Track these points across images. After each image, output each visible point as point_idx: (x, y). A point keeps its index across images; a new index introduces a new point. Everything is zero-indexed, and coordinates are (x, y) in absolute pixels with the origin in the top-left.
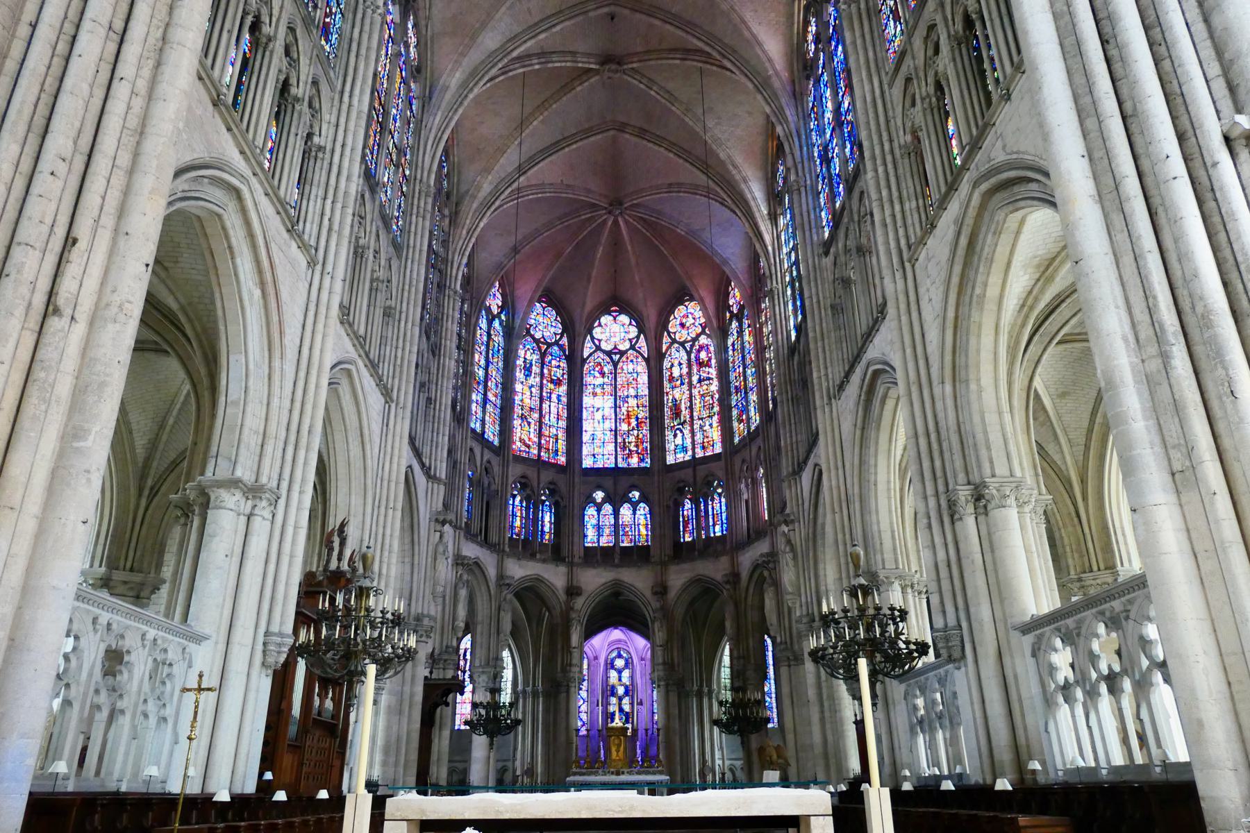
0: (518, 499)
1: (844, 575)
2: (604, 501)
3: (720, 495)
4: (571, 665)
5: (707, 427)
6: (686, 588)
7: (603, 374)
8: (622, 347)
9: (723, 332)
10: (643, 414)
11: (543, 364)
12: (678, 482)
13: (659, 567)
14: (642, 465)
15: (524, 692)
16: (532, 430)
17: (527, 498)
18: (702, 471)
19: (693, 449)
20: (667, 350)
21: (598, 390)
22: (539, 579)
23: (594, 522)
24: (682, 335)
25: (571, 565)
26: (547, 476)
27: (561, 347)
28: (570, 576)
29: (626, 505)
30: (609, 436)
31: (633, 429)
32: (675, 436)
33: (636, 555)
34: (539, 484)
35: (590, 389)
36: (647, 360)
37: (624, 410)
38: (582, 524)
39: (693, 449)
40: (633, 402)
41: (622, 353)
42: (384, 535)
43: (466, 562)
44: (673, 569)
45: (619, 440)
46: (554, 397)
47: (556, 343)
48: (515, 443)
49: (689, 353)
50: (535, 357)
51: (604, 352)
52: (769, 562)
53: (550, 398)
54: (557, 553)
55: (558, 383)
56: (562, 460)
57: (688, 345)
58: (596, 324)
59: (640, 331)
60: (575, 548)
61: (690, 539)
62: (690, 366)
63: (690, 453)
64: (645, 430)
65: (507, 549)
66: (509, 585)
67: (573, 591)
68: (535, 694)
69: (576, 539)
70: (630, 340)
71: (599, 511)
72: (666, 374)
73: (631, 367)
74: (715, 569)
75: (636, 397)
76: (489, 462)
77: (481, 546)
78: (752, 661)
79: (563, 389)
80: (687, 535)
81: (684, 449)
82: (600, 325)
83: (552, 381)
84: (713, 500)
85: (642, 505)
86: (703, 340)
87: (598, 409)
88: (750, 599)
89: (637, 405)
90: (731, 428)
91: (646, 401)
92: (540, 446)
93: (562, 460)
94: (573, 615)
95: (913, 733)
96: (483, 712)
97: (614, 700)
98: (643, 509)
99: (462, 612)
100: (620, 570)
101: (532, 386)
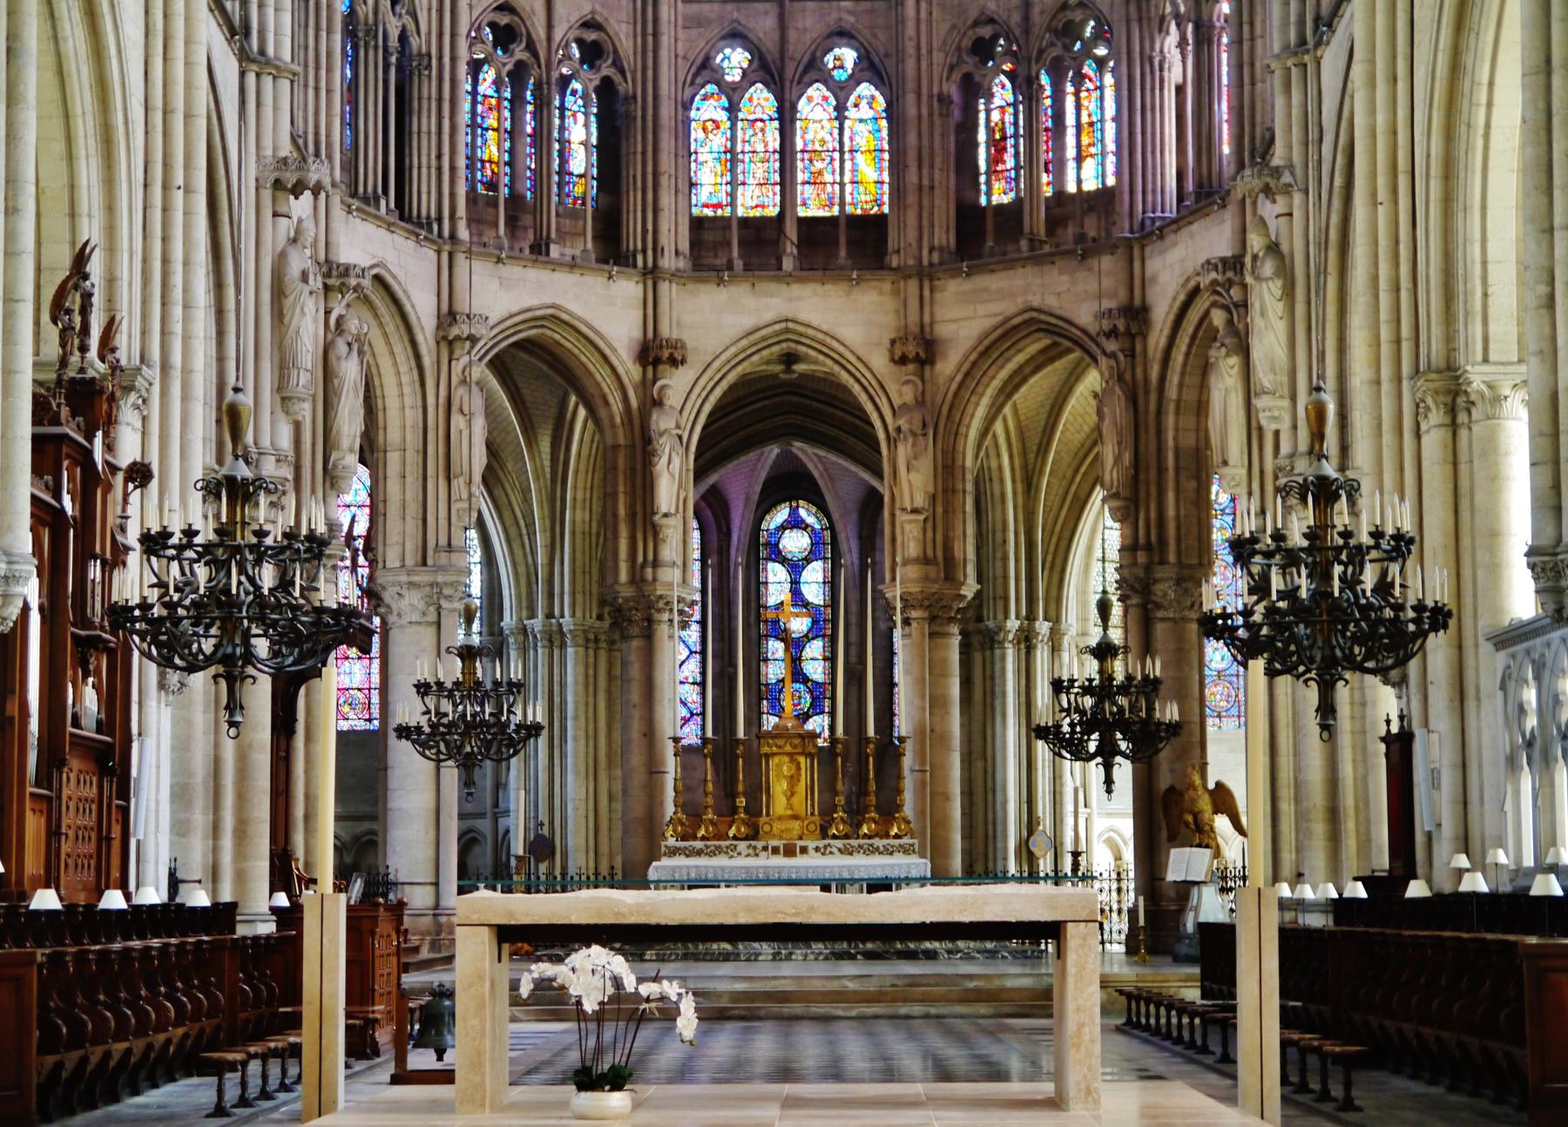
0: (488, 75)
1: (1386, 372)
2: (748, 78)
3: (1101, 63)
4: (656, 564)
12: (976, 24)
13: (913, 285)
17: (517, 76)
22: (555, 318)
23: (718, 141)
25: (652, 275)
28: (652, 308)
29: (817, 91)
34: (550, 26)
38: (686, 153)
42: (166, 261)
43: (353, 282)
52: (1230, 283)
60: (665, 224)
61: (1006, 199)
65: (463, 233)
66: (473, 339)
69: (666, 200)
71: (733, 110)
77: (390, 227)
78: (1172, 558)
80: (998, 186)
84: (1080, 78)
85: (865, 89)
88: (1174, 379)
94: (662, 422)
95: (1512, 763)
96: (446, 706)
97: (776, 648)
98: (868, 101)
99: (350, 424)
100: (796, 289)
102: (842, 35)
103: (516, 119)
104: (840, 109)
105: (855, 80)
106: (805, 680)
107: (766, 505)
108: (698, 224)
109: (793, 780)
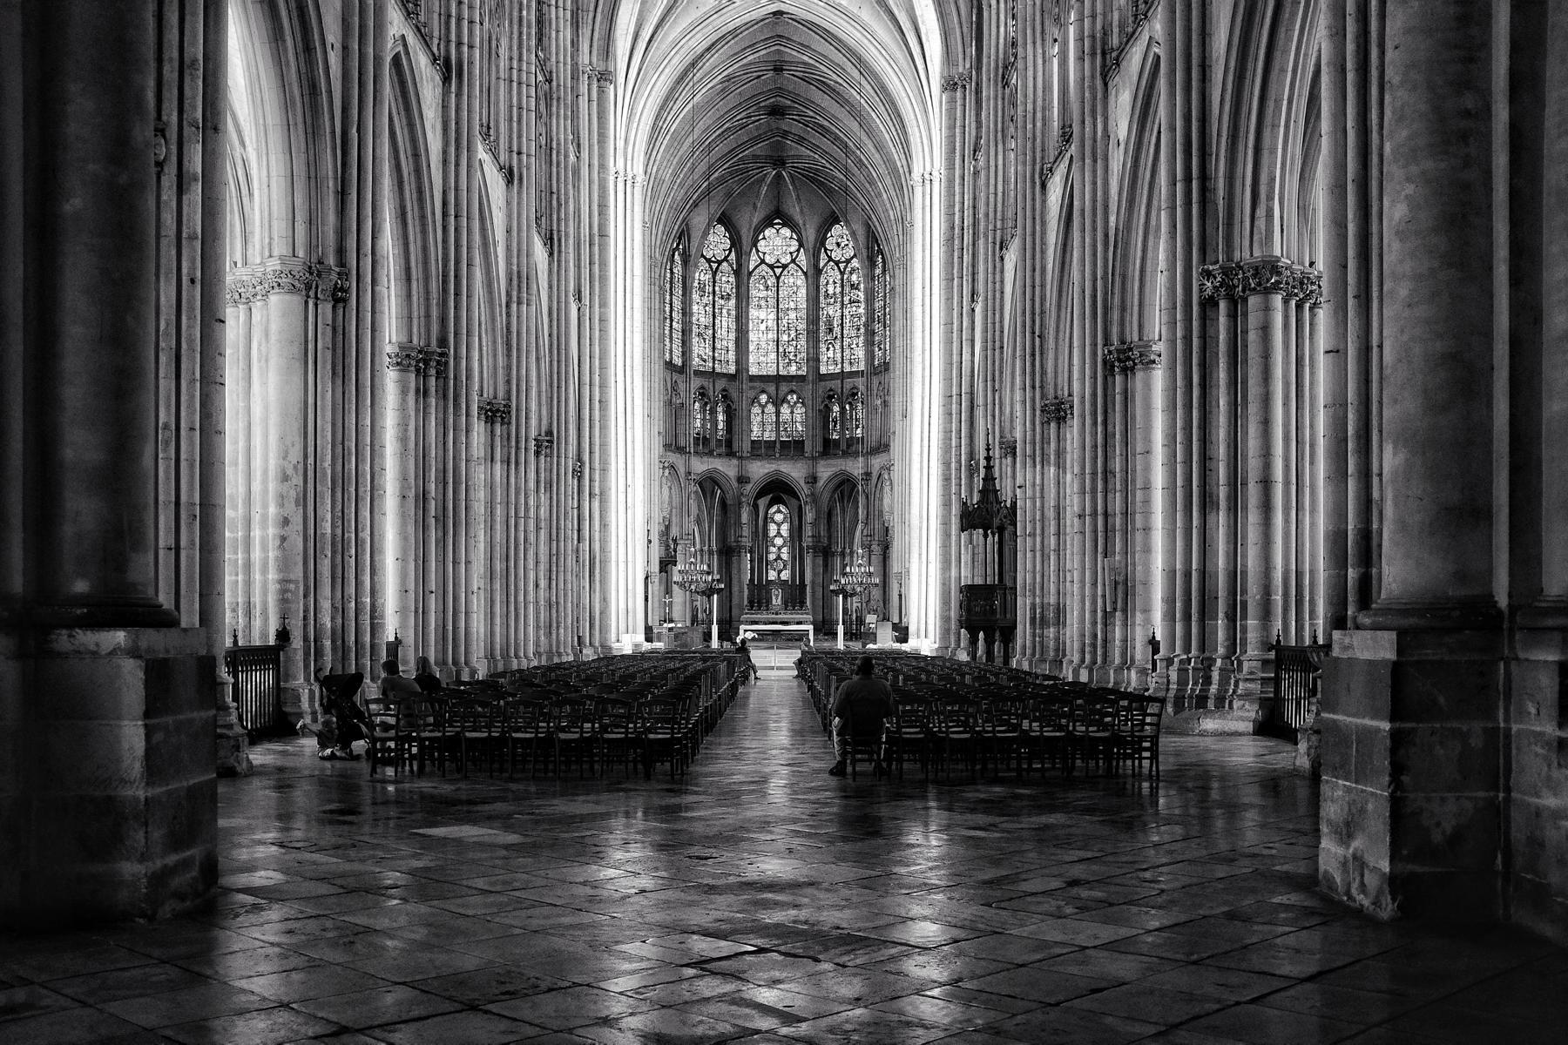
6: (830, 480)
7: (767, 288)
8: (783, 261)
9: (873, 264)
10: (802, 326)
11: (714, 282)
14: (800, 373)
15: (702, 550)
18: (848, 383)
19: (842, 363)
21: (763, 303)
22: (715, 470)
23: (759, 419)
24: (836, 255)
25: (741, 458)
26: (721, 384)
27: (731, 265)
28: (741, 467)
29: (785, 405)
30: (772, 346)
32: (828, 349)
33: (793, 448)
35: (753, 302)
36: (805, 274)
37: (785, 322)
39: (842, 363)
40: (792, 315)
41: (784, 267)
44: (822, 462)
45: (781, 350)
46: (724, 311)
47: (726, 259)
48: (691, 359)
49: (842, 273)
50: (709, 276)
54: (729, 449)
56: (732, 369)
57: (842, 266)
59: (801, 245)
62: (842, 286)
64: (803, 342)
67: (742, 480)
68: (711, 553)
72: (822, 291)
73: (791, 280)
74: (856, 467)
79: (733, 302)
86: (855, 263)
89: (796, 317)
90: (873, 351)
91: (803, 314)
93: (732, 369)
98: (799, 410)
102: (792, 392)
104: (792, 412)
107: (770, 505)
108: (753, 442)
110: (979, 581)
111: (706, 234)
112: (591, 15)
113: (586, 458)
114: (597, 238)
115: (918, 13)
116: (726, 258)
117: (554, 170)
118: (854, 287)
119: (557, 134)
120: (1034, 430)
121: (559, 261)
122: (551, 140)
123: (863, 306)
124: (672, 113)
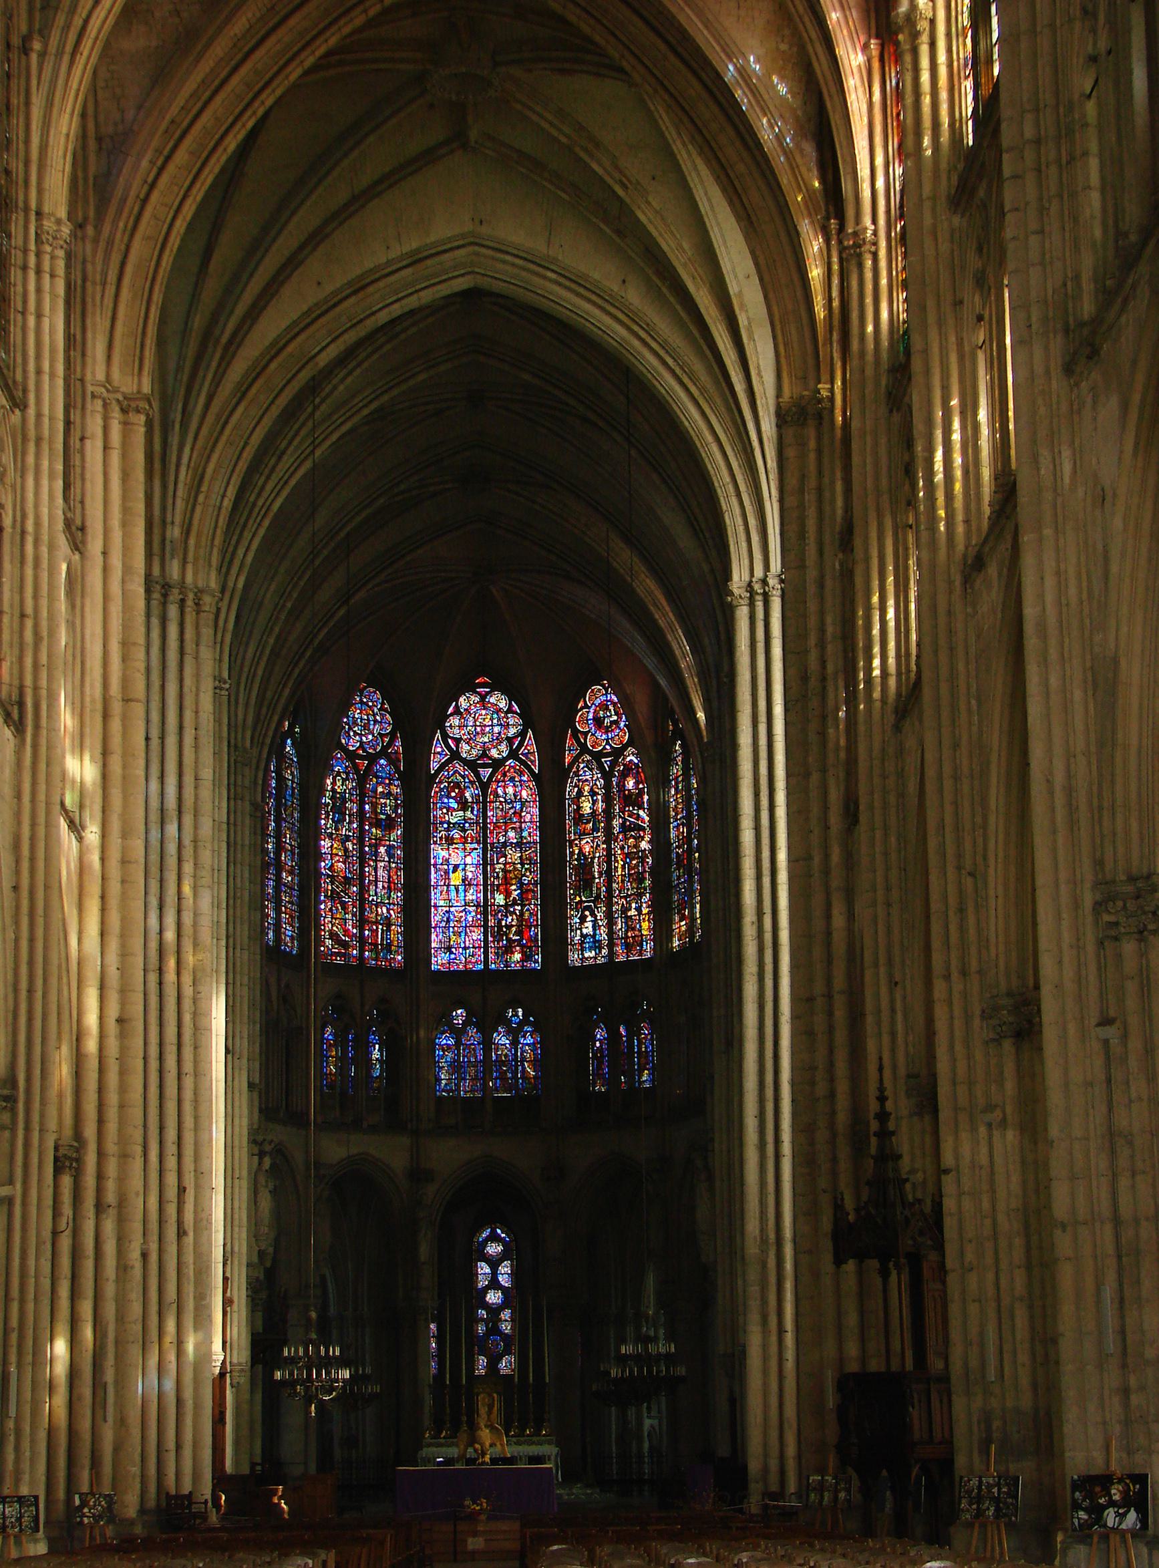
0: (329, 1029)
5: (633, 912)
7: (464, 805)
8: (494, 753)
9: (666, 760)
11: (362, 794)
16: (349, 916)
19: (611, 945)
20: (571, 764)
21: (456, 834)
24: (598, 740)
27: (393, 761)
31: (515, 903)
32: (583, 919)
34: (363, 1005)
40: (514, 855)
41: (497, 764)
46: (382, 850)
47: (383, 753)
48: (320, 942)
49: (607, 776)
51: (465, 762)
53: (376, 854)
55: (389, 825)
58: (451, 710)
62: (608, 799)
63: (605, 952)
64: (534, 906)
67: (419, 1175)
70: (510, 741)
72: (570, 808)
73: (510, 790)
75: (519, 845)
76: (287, 986)
81: (597, 945)
82: (457, 712)
83: (377, 824)
87: (456, 867)
91: (535, 853)
92: (362, 940)
101: (347, 838)
103: (345, 1052)
105: (522, 1024)
106: (500, 1333)
109: (491, 1407)
110: (875, 1365)
111: (346, 705)
112: (111, 290)
113: (90, 1132)
114: (116, 707)
115: (733, 288)
116: (384, 748)
117: (29, 572)
118: (632, 800)
119: (37, 506)
120: (969, 1057)
121: (35, 746)
122: (24, 516)
123: (647, 838)
124: (275, 478)
